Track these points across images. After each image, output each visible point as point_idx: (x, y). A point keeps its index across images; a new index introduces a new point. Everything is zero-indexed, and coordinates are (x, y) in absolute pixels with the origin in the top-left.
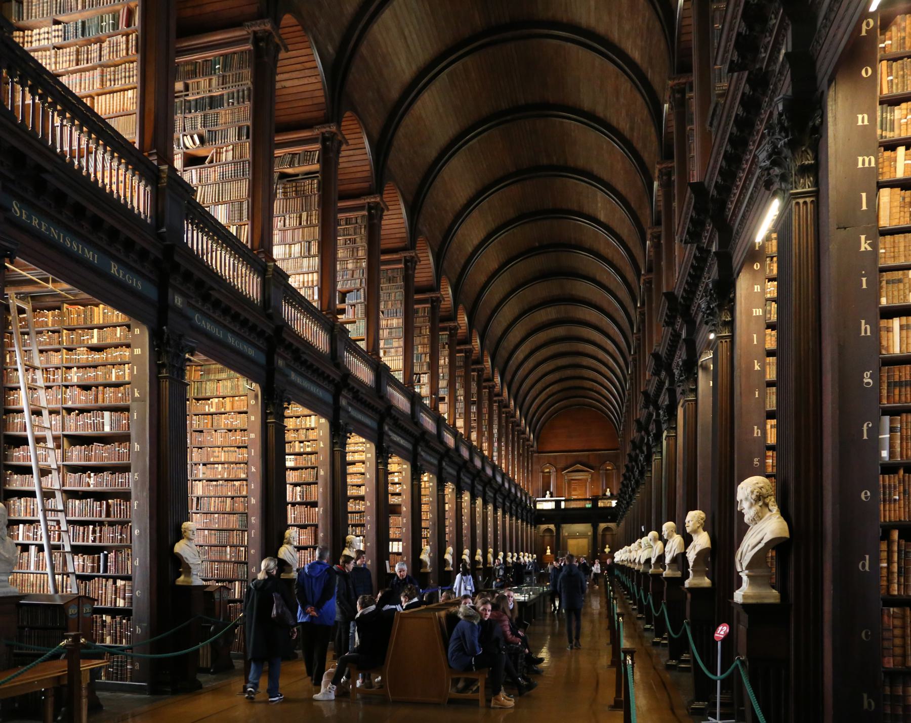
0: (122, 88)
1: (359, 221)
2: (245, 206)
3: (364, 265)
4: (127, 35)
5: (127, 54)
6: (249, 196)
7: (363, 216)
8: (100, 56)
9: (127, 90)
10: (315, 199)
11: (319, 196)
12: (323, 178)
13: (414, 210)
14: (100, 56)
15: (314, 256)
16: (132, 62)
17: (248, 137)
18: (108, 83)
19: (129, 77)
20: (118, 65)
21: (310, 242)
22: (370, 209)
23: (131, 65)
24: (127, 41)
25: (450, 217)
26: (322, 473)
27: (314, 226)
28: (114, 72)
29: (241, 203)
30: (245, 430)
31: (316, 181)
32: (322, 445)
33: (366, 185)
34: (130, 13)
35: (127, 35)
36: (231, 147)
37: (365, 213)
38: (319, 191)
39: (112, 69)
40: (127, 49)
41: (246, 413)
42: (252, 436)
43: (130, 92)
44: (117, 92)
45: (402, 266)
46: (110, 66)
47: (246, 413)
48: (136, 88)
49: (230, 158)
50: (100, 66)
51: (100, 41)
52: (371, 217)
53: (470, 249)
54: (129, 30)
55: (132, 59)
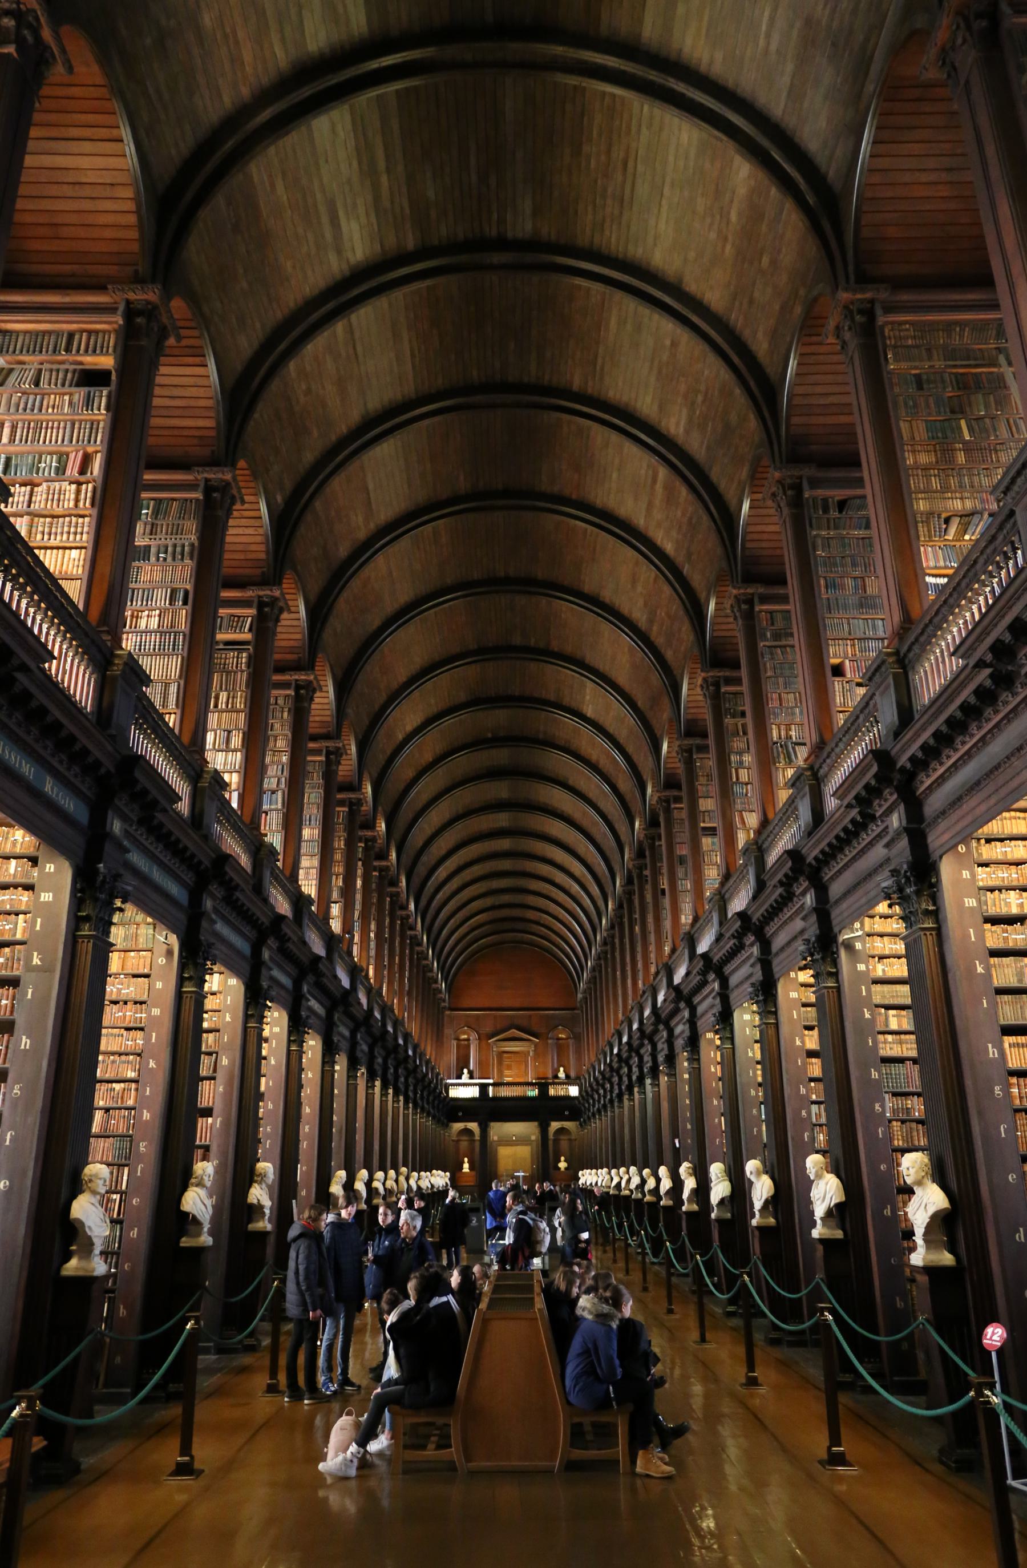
0: (61, 545)
1: (280, 701)
2: (173, 689)
3: (284, 759)
4: (79, 484)
5: (76, 506)
6: (180, 677)
7: (286, 696)
8: (30, 502)
9: (71, 548)
10: (242, 678)
11: (249, 674)
12: (256, 649)
13: (343, 689)
14: (30, 502)
15: (235, 750)
16: (83, 516)
17: (185, 603)
18: (39, 537)
19: (75, 533)
20: (58, 517)
21: (229, 732)
22: (298, 687)
23: (80, 520)
24: (78, 492)
25: (383, 697)
26: (225, 1061)
27: (238, 711)
29: (167, 685)
30: (142, 1003)
31: (244, 655)
32: (228, 1019)
33: (295, 657)
34: (87, 460)
35: (79, 484)
36: (158, 612)
38: (248, 665)
39: (48, 520)
40: (77, 501)
41: (147, 976)
42: (156, 1012)
43: (75, 553)
44: (52, 548)
46: (45, 516)
47: (147, 976)
48: (85, 548)
49: (154, 623)
50: (28, 514)
51: (34, 485)
52: (298, 698)
53: (400, 737)
54: (82, 479)
55: (81, 512)
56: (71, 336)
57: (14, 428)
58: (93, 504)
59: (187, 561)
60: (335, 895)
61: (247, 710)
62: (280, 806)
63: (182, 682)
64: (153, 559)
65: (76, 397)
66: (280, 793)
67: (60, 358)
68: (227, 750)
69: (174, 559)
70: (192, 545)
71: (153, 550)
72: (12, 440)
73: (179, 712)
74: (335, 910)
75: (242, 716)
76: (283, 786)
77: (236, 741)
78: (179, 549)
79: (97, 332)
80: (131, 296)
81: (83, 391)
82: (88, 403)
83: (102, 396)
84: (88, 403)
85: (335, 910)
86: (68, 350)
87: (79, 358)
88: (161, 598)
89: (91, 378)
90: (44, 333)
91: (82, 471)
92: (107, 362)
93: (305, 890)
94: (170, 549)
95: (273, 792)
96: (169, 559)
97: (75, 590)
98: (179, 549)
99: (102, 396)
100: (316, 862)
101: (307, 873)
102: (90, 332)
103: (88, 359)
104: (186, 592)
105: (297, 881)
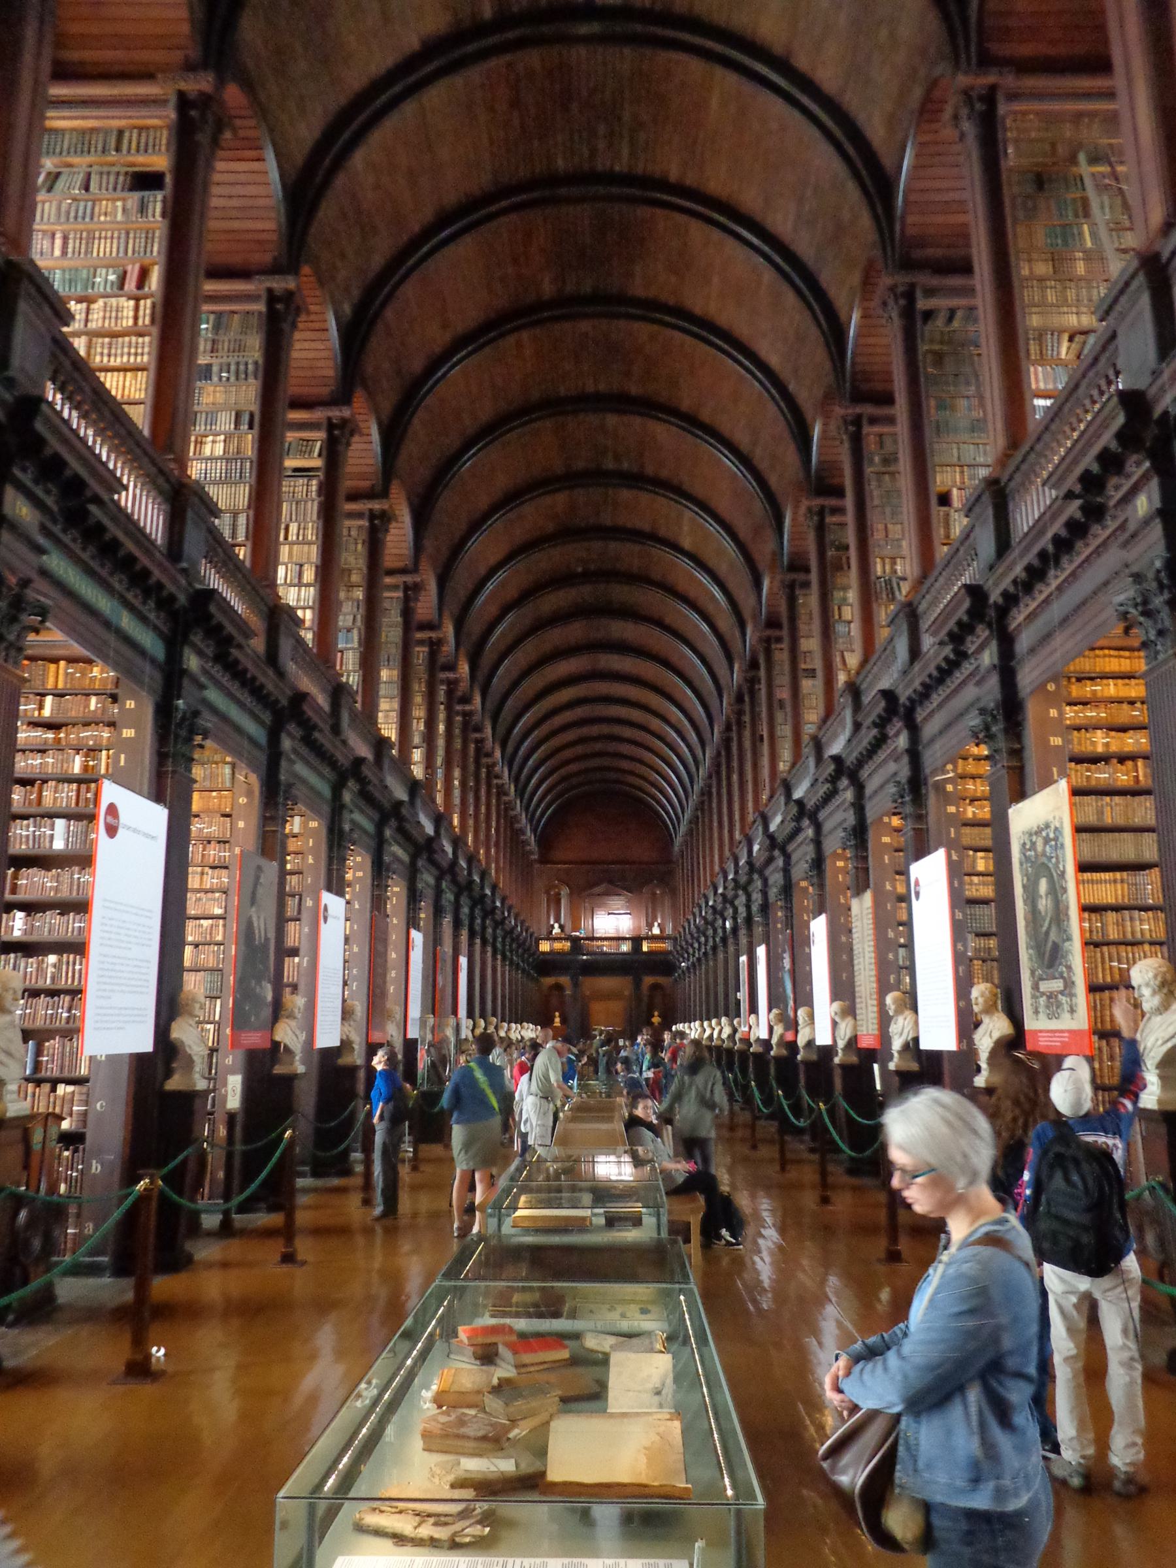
2: (242, 520)
8: (87, 321)
10: (313, 508)
14: (87, 321)
15: (308, 585)
17: (251, 427)
27: (310, 543)
28: (110, 344)
29: (235, 515)
37: (365, 523)
39: (107, 340)
45: (400, 594)
46: (103, 336)
49: (219, 450)
50: (86, 333)
56: (121, 133)
57: (65, 239)
58: (153, 321)
59: (251, 380)
60: (417, 740)
61: (320, 542)
62: (356, 645)
63: (251, 513)
64: (215, 379)
65: (129, 204)
66: (355, 632)
67: (109, 159)
68: (300, 584)
69: (237, 379)
70: (256, 363)
71: (215, 369)
72: (64, 252)
73: (249, 544)
74: (417, 755)
75: (314, 548)
76: (359, 623)
77: (309, 575)
78: (242, 367)
79: (147, 128)
80: (182, 86)
81: (137, 195)
82: (143, 208)
83: (157, 201)
84: (143, 208)
85: (417, 755)
86: (118, 149)
87: (131, 159)
88: (225, 422)
89: (144, 181)
90: (93, 130)
91: (140, 285)
92: (160, 162)
93: (385, 733)
94: (233, 368)
95: (349, 630)
96: (232, 379)
97: (140, 416)
98: (242, 367)
99: (157, 201)
100: (396, 705)
101: (386, 717)
102: (141, 129)
103: (140, 159)
104: (252, 415)
105: (376, 723)
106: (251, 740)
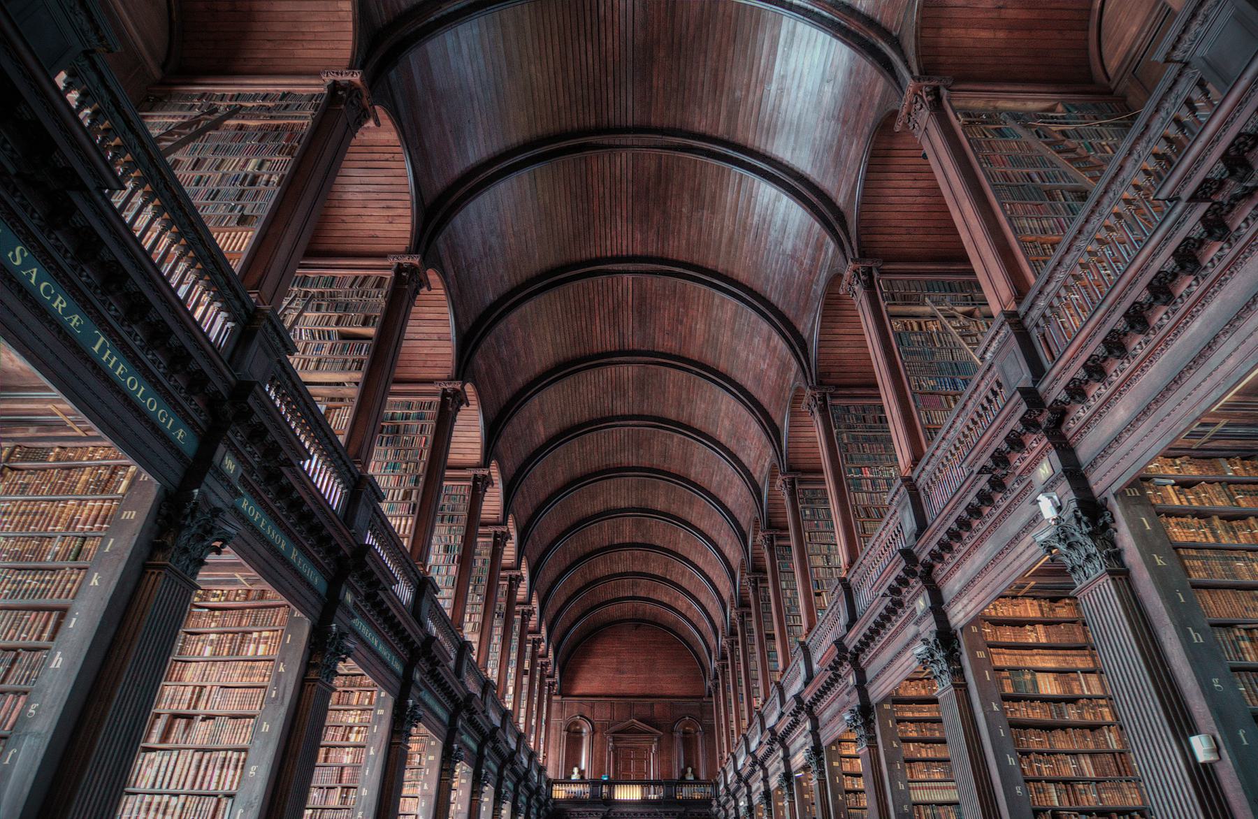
106: (393, 671)
